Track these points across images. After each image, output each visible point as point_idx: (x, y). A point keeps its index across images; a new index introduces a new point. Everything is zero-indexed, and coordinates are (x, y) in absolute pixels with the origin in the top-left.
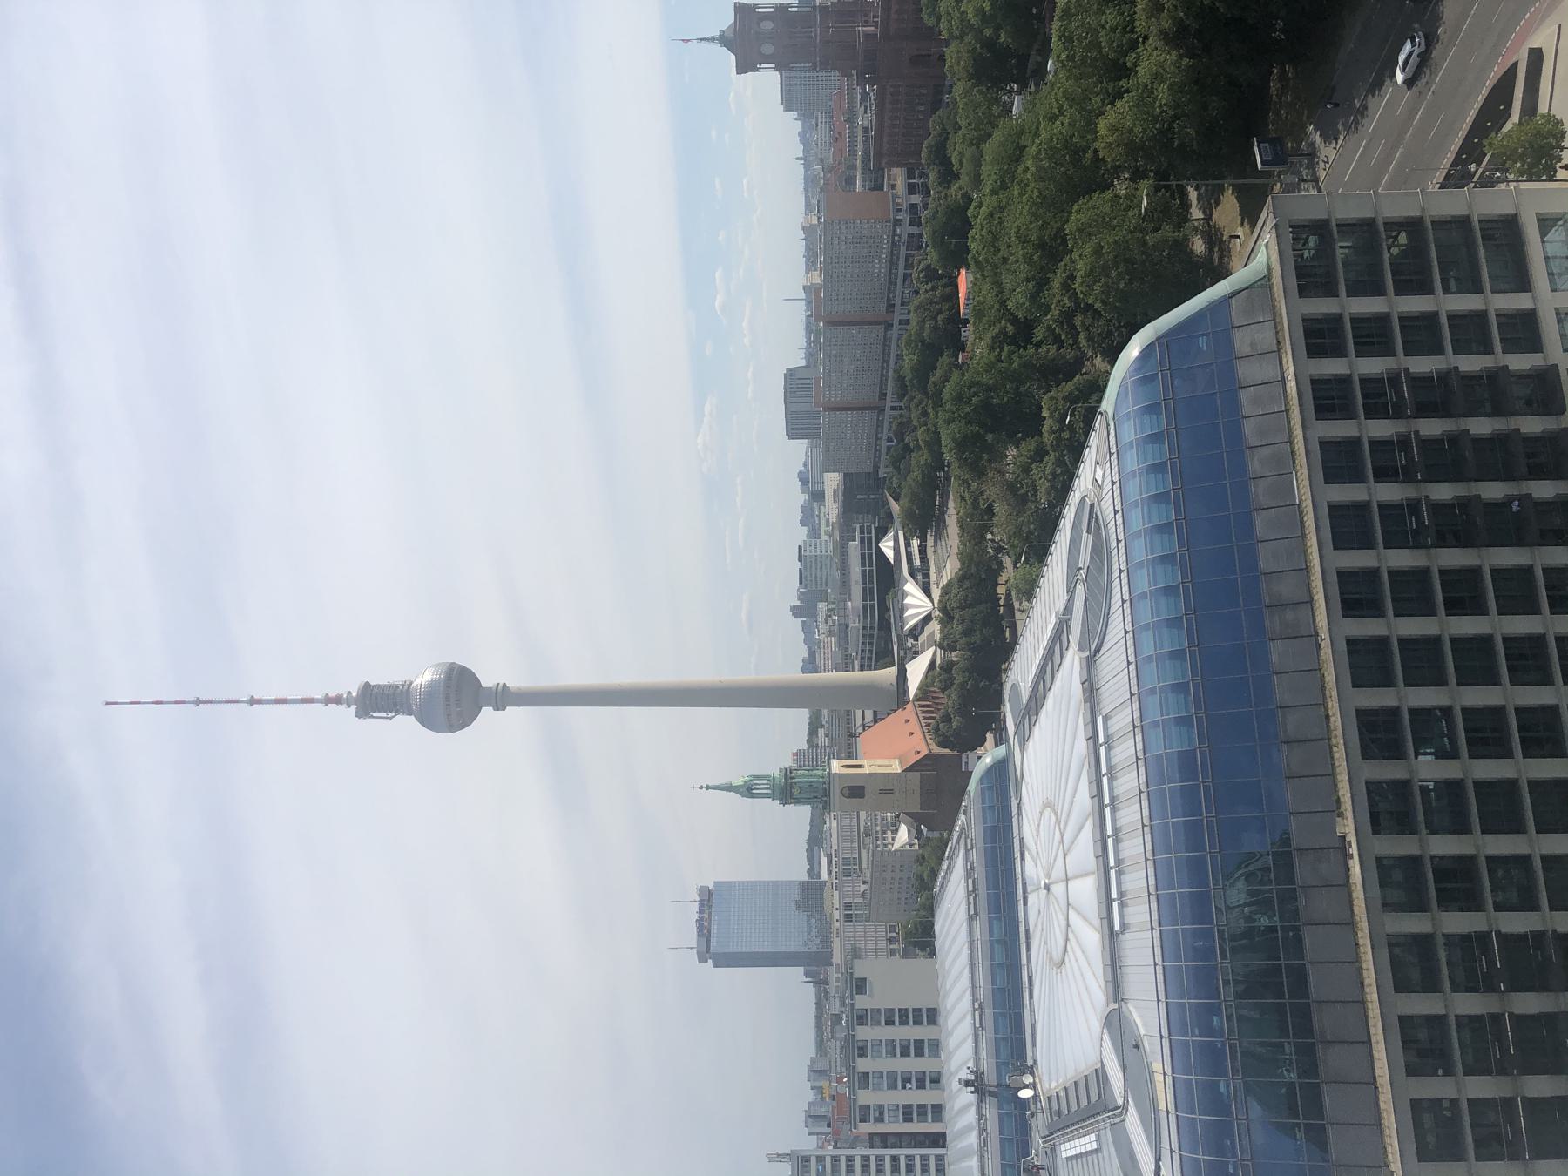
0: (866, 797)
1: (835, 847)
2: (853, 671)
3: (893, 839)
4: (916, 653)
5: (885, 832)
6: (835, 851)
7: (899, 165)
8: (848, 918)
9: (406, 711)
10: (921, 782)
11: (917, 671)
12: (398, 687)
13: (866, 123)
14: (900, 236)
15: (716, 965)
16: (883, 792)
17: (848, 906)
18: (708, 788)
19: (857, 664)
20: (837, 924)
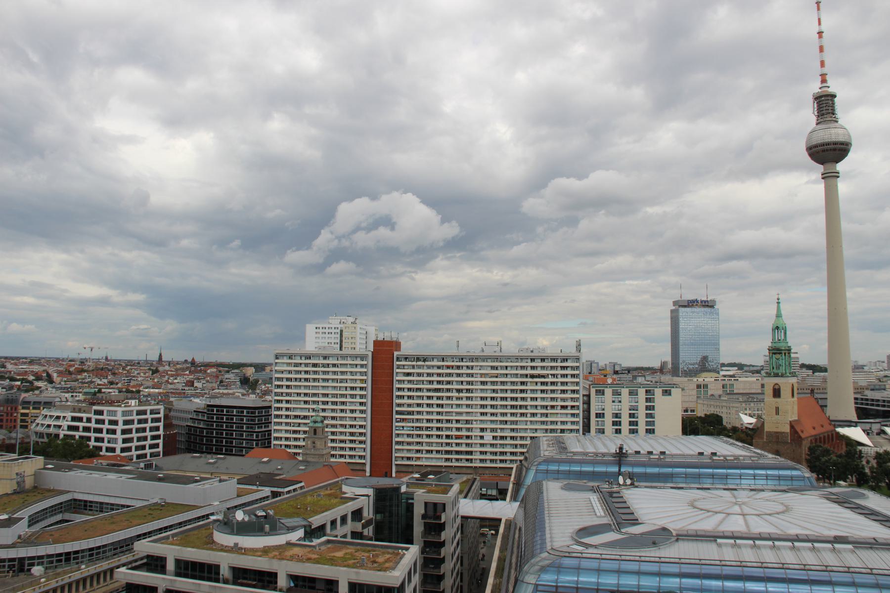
0: (774, 399)
1: (740, 379)
2: (854, 393)
3: (746, 414)
4: (868, 434)
8: (699, 386)
9: (819, 121)
10: (783, 432)
11: (856, 433)
12: (834, 115)
15: (672, 311)
16: (777, 409)
17: (706, 386)
19: (859, 396)
20: (695, 379)
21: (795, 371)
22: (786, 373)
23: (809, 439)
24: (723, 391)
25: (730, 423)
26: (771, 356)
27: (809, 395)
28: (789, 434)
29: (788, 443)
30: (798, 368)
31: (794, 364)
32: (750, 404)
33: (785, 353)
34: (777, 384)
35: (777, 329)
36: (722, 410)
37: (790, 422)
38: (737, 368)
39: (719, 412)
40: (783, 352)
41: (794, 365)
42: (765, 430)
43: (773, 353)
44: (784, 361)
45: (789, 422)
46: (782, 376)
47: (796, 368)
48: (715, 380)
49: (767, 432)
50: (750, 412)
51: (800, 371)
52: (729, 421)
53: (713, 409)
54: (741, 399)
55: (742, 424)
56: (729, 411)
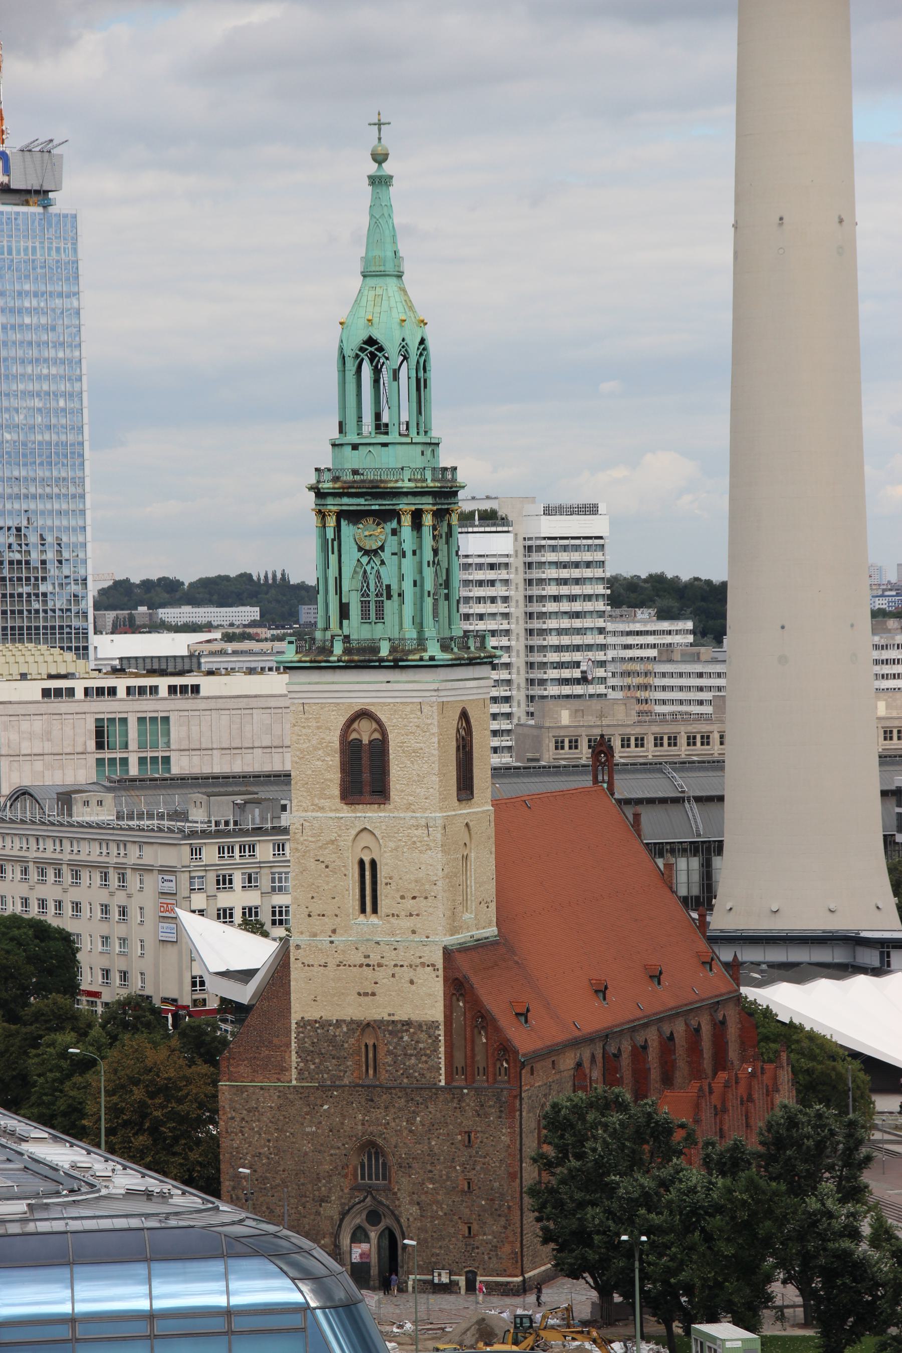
0: (347, 812)
1: (209, 686)
3: (225, 915)
5: (250, 881)
6: (196, 689)
10: (408, 1023)
18: (379, 182)
21: (481, 626)
22: (421, 643)
23: (568, 1062)
24: (100, 762)
25: (124, 975)
26: (330, 534)
27: (586, 781)
28: (442, 1032)
29: (433, 1087)
30: (600, 606)
31: (577, 581)
32: (252, 848)
33: (417, 516)
34: (363, 714)
35: (372, 356)
36: (75, 894)
37: (448, 953)
38: (252, 613)
39: (59, 904)
40: (405, 505)
41: (576, 590)
42: (295, 1017)
43: (340, 515)
44: (408, 564)
45: (440, 964)
46: (397, 663)
47: (588, 606)
48: (46, 693)
49: (303, 1024)
50: (252, 898)
51: (610, 627)
52: (120, 964)
53: (22, 890)
54: (198, 816)
55: (198, 983)
56: (120, 898)
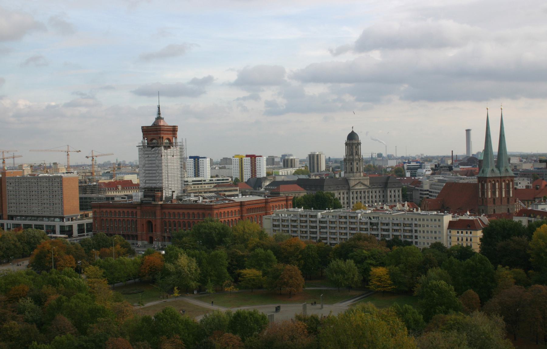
7: (94, 218)
13: (116, 199)
14: (54, 221)
